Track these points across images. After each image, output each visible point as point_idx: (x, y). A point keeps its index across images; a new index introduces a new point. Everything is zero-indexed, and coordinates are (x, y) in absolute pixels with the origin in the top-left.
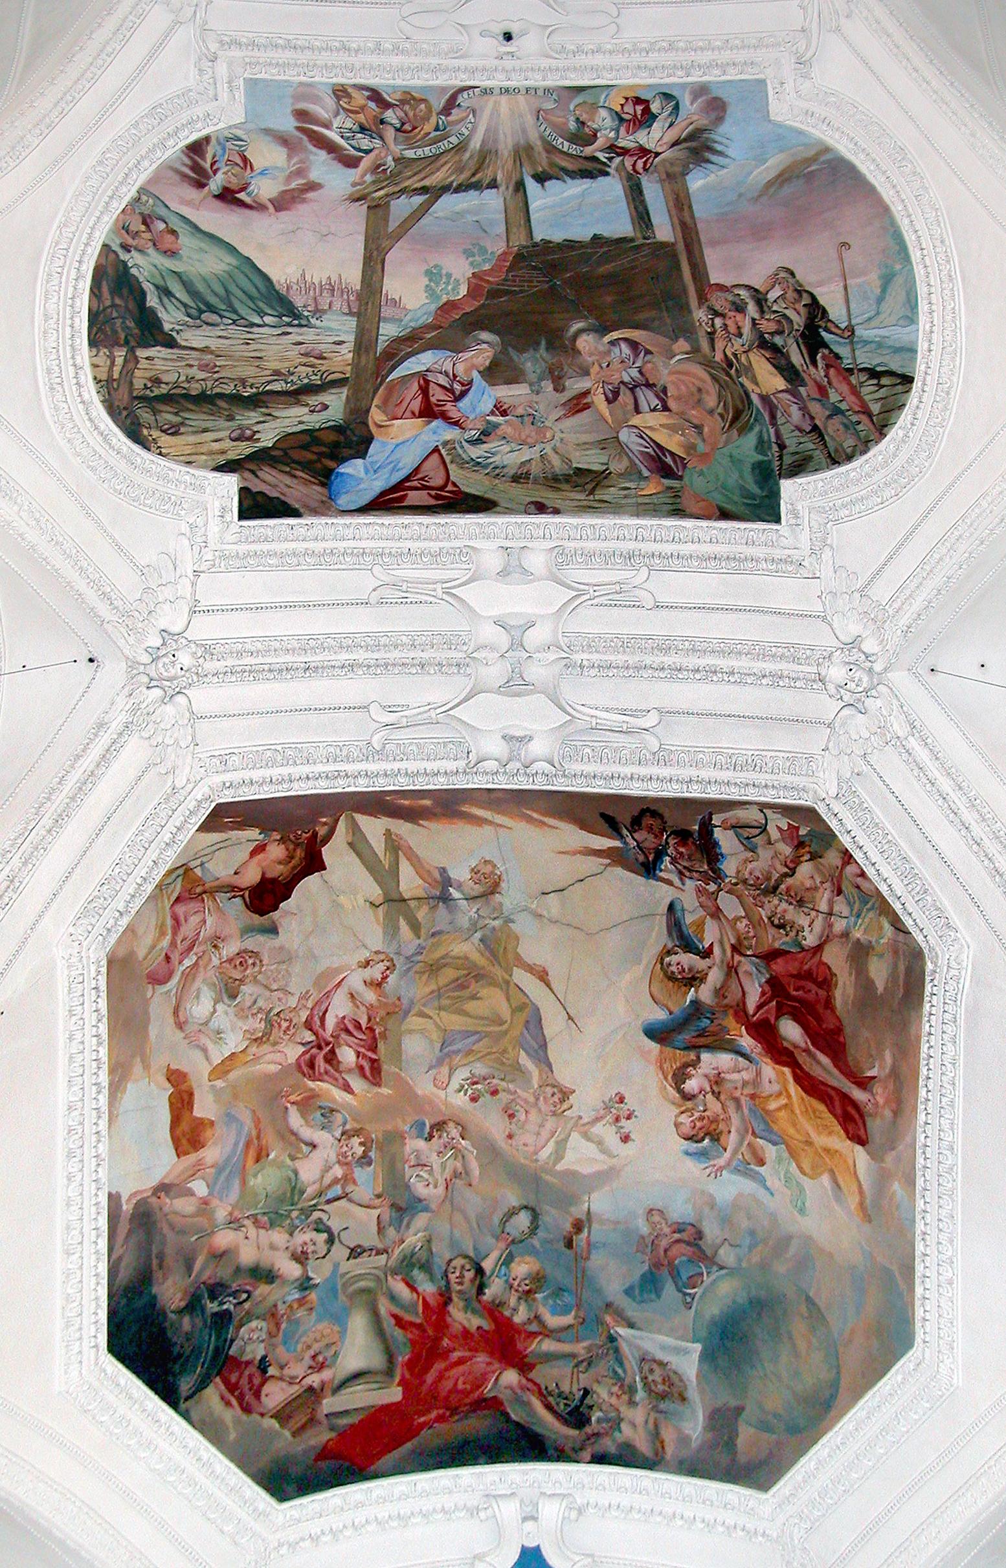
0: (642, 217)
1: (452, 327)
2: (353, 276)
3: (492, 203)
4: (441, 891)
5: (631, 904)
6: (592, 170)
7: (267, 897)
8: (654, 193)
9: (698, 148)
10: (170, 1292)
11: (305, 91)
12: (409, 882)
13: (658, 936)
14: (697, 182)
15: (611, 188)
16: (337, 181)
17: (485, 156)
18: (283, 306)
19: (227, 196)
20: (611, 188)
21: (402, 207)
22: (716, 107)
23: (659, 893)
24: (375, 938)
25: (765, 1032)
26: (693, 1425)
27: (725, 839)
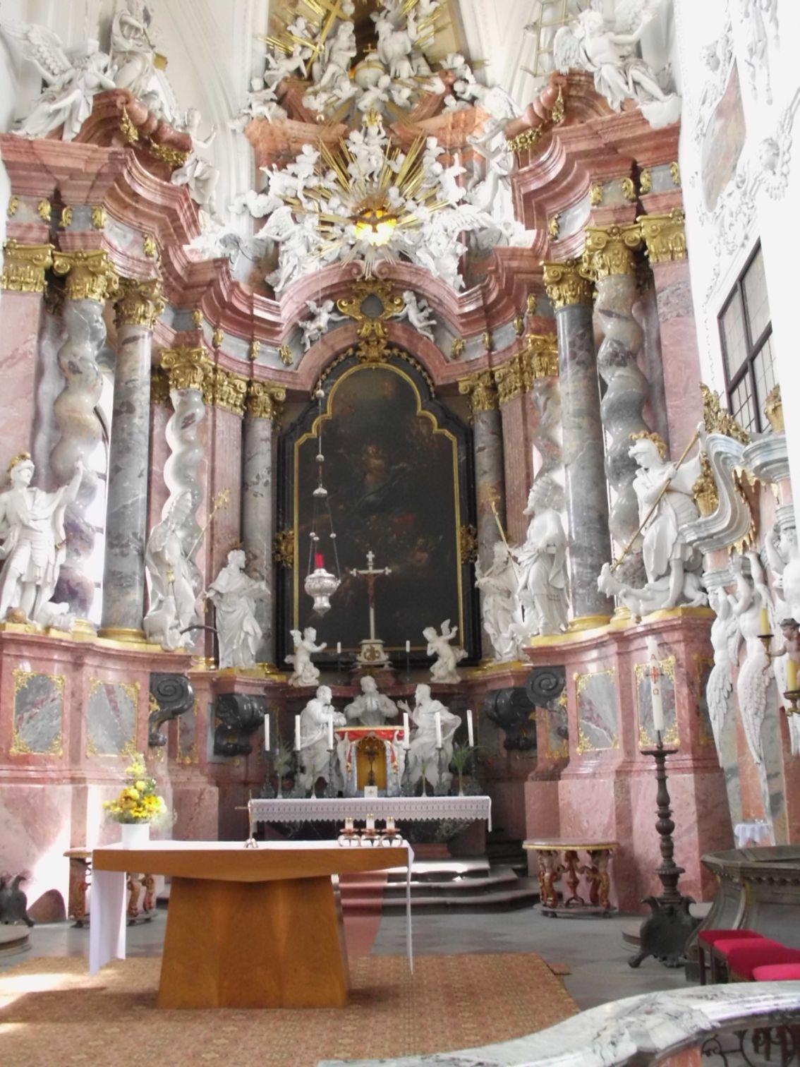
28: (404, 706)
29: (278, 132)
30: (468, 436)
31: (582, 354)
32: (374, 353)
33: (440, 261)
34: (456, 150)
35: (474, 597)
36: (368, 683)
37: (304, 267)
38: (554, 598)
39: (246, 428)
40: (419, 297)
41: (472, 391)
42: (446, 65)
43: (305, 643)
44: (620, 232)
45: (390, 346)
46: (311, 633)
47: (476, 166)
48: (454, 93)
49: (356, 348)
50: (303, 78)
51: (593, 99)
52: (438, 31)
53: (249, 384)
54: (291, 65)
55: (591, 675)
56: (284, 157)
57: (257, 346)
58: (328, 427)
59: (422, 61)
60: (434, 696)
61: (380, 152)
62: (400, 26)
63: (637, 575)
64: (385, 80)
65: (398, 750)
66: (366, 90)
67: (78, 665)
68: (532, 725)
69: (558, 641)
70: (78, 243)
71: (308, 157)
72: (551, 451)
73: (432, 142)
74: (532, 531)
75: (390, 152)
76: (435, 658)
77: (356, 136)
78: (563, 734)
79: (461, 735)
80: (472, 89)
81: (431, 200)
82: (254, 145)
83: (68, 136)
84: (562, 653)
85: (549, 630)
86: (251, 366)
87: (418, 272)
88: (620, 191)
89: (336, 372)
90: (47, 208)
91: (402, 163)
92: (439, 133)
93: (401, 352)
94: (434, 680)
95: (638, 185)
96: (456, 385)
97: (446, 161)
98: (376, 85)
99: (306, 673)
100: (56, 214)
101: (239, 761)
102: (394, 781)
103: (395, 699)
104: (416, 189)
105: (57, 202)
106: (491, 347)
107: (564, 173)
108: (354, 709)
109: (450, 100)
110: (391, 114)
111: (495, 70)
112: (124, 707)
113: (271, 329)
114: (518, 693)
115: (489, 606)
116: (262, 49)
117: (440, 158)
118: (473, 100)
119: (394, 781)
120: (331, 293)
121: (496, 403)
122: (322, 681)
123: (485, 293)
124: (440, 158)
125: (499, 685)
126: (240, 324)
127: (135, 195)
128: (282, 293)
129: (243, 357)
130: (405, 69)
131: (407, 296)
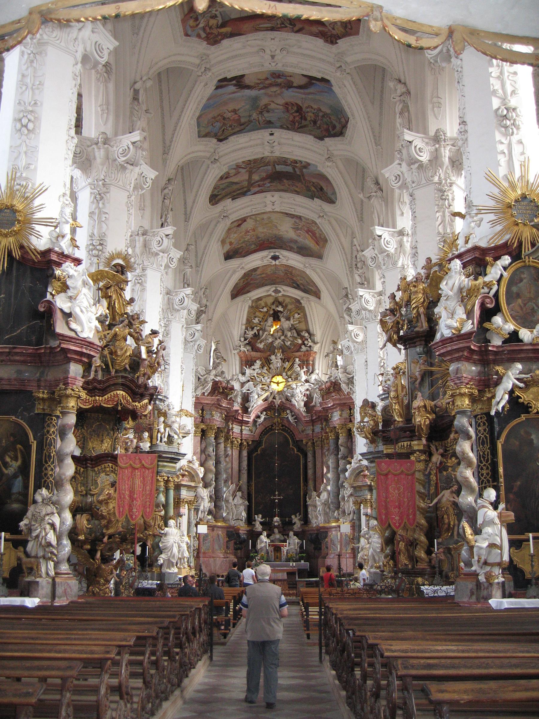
0: (295, 171)
1: (263, 179)
2: (246, 177)
3: (270, 168)
4: (263, 219)
6: (287, 165)
7: (239, 226)
8: (296, 169)
10: (230, 254)
12: (258, 219)
14: (304, 170)
16: (244, 171)
17: (268, 162)
18: (236, 183)
19: (226, 178)
22: (309, 164)
23: (294, 220)
26: (295, 250)
27: (304, 220)
28: (286, 537)
29: (248, 356)
30: (305, 456)
31: (336, 452)
33: (299, 402)
35: (306, 507)
36: (276, 530)
37: (257, 403)
38: (326, 514)
40: (291, 412)
41: (307, 443)
43: (259, 518)
44: (346, 425)
45: (283, 426)
46: (260, 516)
47: (311, 367)
48: (304, 344)
49: (272, 426)
50: (256, 336)
52: (299, 322)
53: (241, 440)
54: (253, 333)
55: (333, 534)
56: (250, 363)
57: (243, 427)
58: (263, 450)
59: (294, 331)
60: (294, 535)
61: (280, 360)
63: (344, 512)
64: (283, 338)
65: (285, 550)
66: (276, 339)
67: (213, 530)
68: (320, 544)
69: (327, 525)
70: (208, 421)
71: (258, 363)
72: (328, 468)
73: (297, 360)
74: (321, 497)
75: (283, 360)
76: (295, 523)
77: (273, 357)
78: (327, 548)
79: (301, 547)
80: (310, 344)
81: (296, 379)
82: (241, 358)
83: (206, 394)
84: (328, 528)
85: (325, 522)
86: (242, 434)
87: (292, 405)
88: (346, 414)
89: (265, 434)
90: (200, 412)
91: (287, 365)
92: (299, 357)
93: (286, 428)
94: (295, 530)
95: (351, 413)
96: (302, 441)
98: (280, 338)
99: (259, 527)
101: (239, 551)
102: (284, 557)
103: (283, 535)
104: (292, 374)
105: (203, 410)
106: (313, 431)
108: (272, 537)
109: (303, 347)
110: (284, 349)
111: (318, 338)
112: (221, 539)
113: (247, 422)
114: (317, 535)
115: (310, 509)
116: (244, 327)
118: (310, 346)
119: (284, 557)
120: (265, 410)
121: (314, 448)
122: (264, 530)
123: (312, 416)
125: (312, 532)
126: (239, 423)
127: (221, 406)
128: (251, 411)
129: (239, 431)
130: (289, 334)
131: (288, 411)
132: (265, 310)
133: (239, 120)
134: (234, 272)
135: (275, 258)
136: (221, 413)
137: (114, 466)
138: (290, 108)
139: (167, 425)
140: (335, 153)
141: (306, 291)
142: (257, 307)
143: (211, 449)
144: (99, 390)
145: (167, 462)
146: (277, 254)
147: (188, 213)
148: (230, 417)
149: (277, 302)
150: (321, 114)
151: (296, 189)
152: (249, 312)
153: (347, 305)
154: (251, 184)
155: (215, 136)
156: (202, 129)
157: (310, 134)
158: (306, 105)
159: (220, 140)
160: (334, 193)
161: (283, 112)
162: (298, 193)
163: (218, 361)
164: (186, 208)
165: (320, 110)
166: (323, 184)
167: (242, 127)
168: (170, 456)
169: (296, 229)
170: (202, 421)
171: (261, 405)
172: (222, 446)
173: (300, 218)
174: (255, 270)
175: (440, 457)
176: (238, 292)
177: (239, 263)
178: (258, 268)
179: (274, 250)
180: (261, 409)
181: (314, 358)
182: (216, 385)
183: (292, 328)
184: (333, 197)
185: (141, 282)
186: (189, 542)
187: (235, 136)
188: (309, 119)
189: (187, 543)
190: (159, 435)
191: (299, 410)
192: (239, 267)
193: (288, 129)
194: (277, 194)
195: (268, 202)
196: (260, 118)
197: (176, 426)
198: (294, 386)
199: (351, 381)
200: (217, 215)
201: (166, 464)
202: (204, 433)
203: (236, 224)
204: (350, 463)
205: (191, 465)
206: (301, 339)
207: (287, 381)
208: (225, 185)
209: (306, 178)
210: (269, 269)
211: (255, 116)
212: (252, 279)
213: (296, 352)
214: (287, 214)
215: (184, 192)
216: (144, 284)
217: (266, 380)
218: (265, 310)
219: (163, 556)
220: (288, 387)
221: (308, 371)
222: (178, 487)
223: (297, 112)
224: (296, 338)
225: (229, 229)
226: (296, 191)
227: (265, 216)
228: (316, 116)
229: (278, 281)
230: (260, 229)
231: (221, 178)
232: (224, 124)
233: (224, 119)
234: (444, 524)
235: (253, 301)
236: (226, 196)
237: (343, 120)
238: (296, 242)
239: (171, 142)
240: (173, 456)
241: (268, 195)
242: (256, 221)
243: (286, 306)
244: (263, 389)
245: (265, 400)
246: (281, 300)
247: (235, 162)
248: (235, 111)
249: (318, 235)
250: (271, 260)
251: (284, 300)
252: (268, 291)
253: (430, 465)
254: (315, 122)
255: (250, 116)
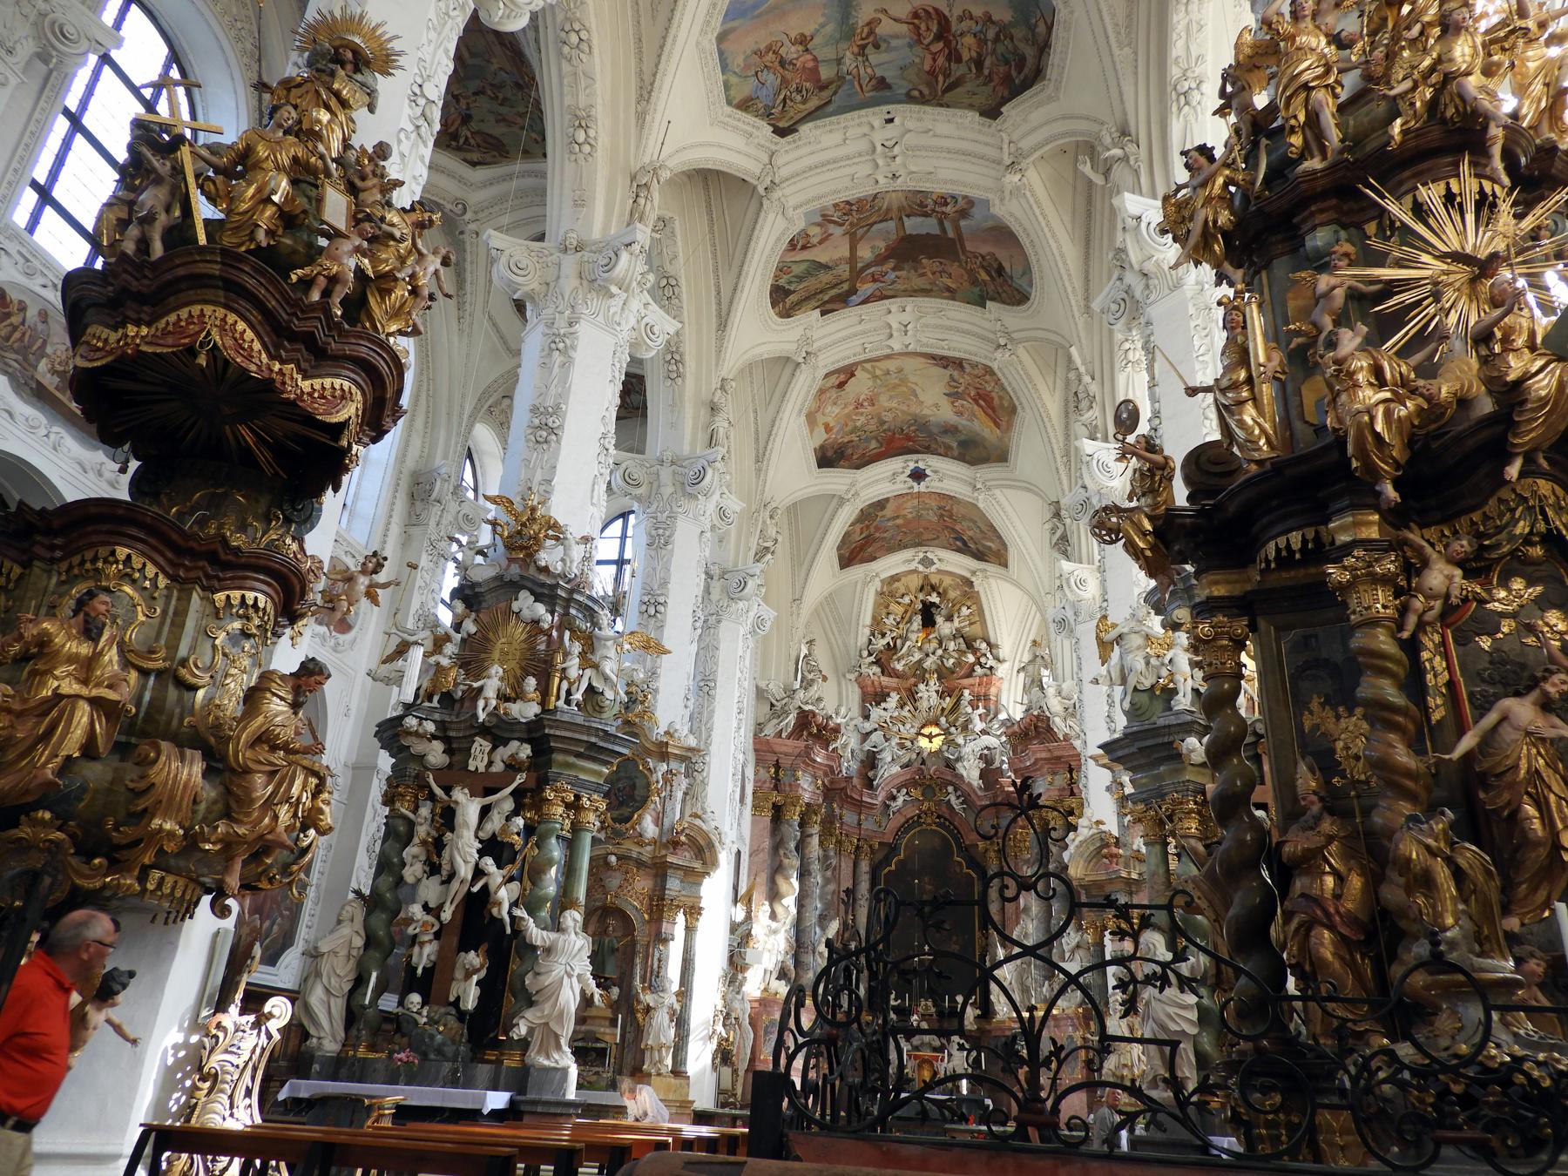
0: (944, 230)
1: (880, 260)
2: (847, 254)
3: (891, 225)
5: (940, 375)
6: (926, 215)
7: (841, 385)
8: (947, 224)
9: (964, 214)
10: (830, 453)
11: (824, 208)
12: (878, 372)
13: (947, 379)
14: (963, 223)
15: (933, 221)
16: (838, 231)
17: (888, 210)
18: (826, 267)
19: (804, 248)
20: (933, 221)
21: (860, 232)
22: (971, 202)
23: (948, 372)
24: (870, 383)
25: (976, 401)
26: (956, 453)
32: (929, 820)
33: (970, 771)
34: (981, 698)
39: (856, 865)
42: (977, 644)
45: (939, 817)
47: (992, 707)
50: (891, 649)
51: (1049, 729)
54: (884, 642)
56: (880, 697)
58: (901, 863)
62: (949, 618)
71: (893, 699)
73: (966, 692)
75: (941, 695)
77: (922, 687)
80: (991, 662)
88: (1061, 780)
93: (946, 819)
97: (975, 708)
100: (777, 772)
105: (777, 766)
107: (1035, 763)
109: (977, 668)
110: (943, 673)
111: (1002, 653)
116: (867, 631)
117: (970, 703)
124: (970, 703)
130: (952, 646)
131: (950, 789)
132: (907, 600)
133: (815, 71)
134: (842, 501)
135: (918, 475)
136: (815, 777)
137: (137, 562)
138: (923, 27)
139: (587, 662)
140: (1025, 144)
141: (980, 556)
142: (892, 595)
143: (792, 845)
144: (140, 298)
145: (579, 755)
146: (921, 465)
147: (724, 313)
148: (834, 791)
149: (928, 586)
150: (991, 34)
151: (949, 282)
152: (877, 605)
153: (1059, 533)
154: (857, 274)
155: (767, 115)
156: (734, 80)
157: (971, 107)
158: (957, 12)
159: (781, 132)
160: (1027, 270)
161: (910, 46)
162: (951, 294)
163: (810, 676)
164: (719, 303)
165: (988, 19)
166: (1003, 255)
167: (826, 94)
168: (585, 738)
169: (954, 396)
170: (776, 788)
171: (897, 776)
172: (815, 841)
173: (958, 364)
174: (881, 504)
175: (1458, 572)
176: (854, 553)
177: (849, 481)
178: (887, 500)
179: (915, 457)
180: (896, 782)
181: (999, 690)
182: (805, 720)
183: (958, 634)
184: (1021, 282)
185: (560, 346)
186: (677, 1007)
187: (810, 125)
188: (966, 56)
189: (672, 1012)
190: (565, 685)
191: (969, 784)
192: (848, 491)
193: (923, 100)
194: (910, 303)
195: (895, 325)
196: (862, 71)
197: (609, 667)
198: (960, 740)
199: (1072, 711)
200: (794, 346)
201: (572, 759)
202: (778, 814)
203: (834, 380)
204: (1074, 828)
205: (698, 822)
206: (974, 653)
207: (947, 732)
208: (803, 267)
209: (969, 247)
210: (909, 504)
211: (849, 62)
212: (877, 529)
213: (963, 676)
214: (933, 357)
215: (716, 270)
216: (572, 353)
217: (908, 730)
218: (907, 600)
219: (530, 1014)
220: (950, 743)
221: (987, 715)
222: (660, 870)
223: (938, 37)
224: (963, 653)
225: (822, 391)
226: (949, 289)
227: (892, 365)
228: (982, 42)
229: (925, 537)
230: (884, 401)
231: (792, 245)
232: (785, 82)
233: (782, 63)
234: (1526, 842)
235: (882, 581)
236: (807, 299)
237: (1041, 28)
238: (950, 430)
239: (654, 75)
240: (593, 740)
241: (893, 305)
242: (875, 377)
243: (945, 591)
244: (902, 746)
245: (907, 766)
246: (934, 580)
247: (817, 205)
248: (803, 41)
249: (996, 402)
250: (910, 482)
251: (941, 581)
252: (909, 561)
253: (1418, 603)
254: (979, 64)
255: (839, 61)
